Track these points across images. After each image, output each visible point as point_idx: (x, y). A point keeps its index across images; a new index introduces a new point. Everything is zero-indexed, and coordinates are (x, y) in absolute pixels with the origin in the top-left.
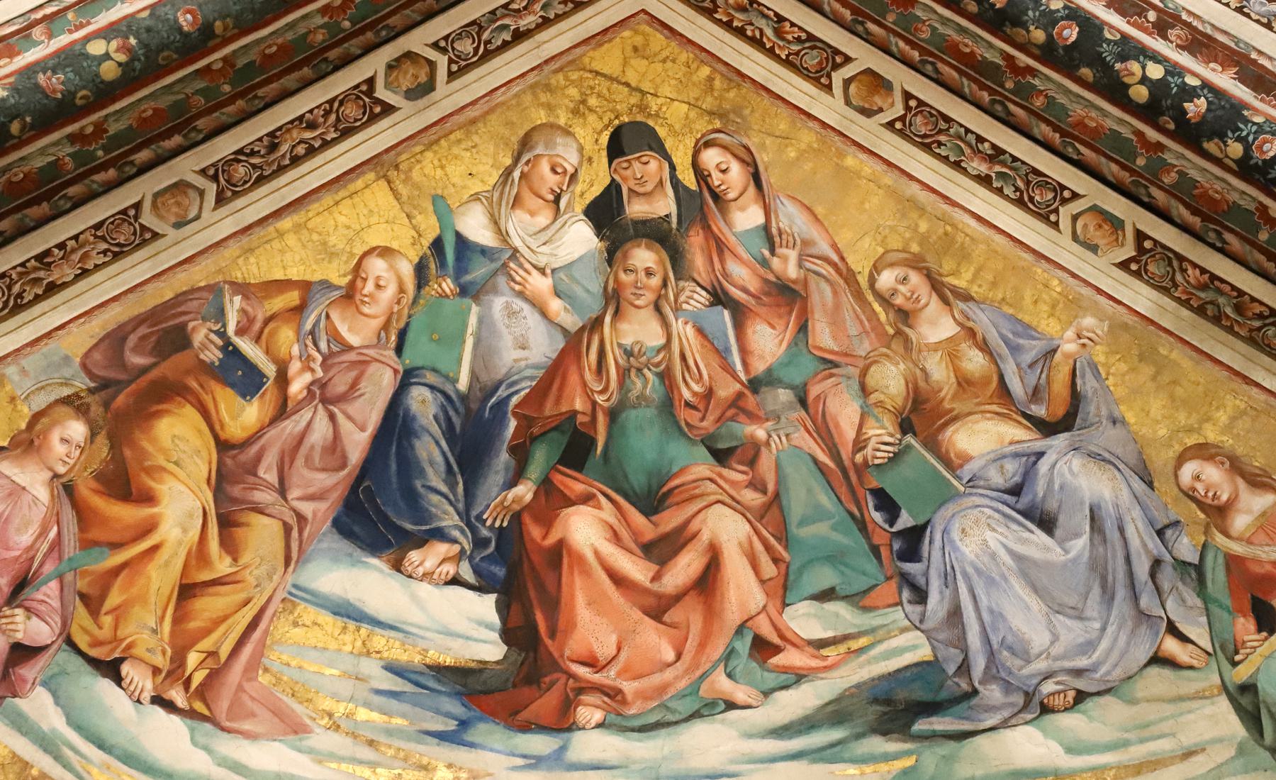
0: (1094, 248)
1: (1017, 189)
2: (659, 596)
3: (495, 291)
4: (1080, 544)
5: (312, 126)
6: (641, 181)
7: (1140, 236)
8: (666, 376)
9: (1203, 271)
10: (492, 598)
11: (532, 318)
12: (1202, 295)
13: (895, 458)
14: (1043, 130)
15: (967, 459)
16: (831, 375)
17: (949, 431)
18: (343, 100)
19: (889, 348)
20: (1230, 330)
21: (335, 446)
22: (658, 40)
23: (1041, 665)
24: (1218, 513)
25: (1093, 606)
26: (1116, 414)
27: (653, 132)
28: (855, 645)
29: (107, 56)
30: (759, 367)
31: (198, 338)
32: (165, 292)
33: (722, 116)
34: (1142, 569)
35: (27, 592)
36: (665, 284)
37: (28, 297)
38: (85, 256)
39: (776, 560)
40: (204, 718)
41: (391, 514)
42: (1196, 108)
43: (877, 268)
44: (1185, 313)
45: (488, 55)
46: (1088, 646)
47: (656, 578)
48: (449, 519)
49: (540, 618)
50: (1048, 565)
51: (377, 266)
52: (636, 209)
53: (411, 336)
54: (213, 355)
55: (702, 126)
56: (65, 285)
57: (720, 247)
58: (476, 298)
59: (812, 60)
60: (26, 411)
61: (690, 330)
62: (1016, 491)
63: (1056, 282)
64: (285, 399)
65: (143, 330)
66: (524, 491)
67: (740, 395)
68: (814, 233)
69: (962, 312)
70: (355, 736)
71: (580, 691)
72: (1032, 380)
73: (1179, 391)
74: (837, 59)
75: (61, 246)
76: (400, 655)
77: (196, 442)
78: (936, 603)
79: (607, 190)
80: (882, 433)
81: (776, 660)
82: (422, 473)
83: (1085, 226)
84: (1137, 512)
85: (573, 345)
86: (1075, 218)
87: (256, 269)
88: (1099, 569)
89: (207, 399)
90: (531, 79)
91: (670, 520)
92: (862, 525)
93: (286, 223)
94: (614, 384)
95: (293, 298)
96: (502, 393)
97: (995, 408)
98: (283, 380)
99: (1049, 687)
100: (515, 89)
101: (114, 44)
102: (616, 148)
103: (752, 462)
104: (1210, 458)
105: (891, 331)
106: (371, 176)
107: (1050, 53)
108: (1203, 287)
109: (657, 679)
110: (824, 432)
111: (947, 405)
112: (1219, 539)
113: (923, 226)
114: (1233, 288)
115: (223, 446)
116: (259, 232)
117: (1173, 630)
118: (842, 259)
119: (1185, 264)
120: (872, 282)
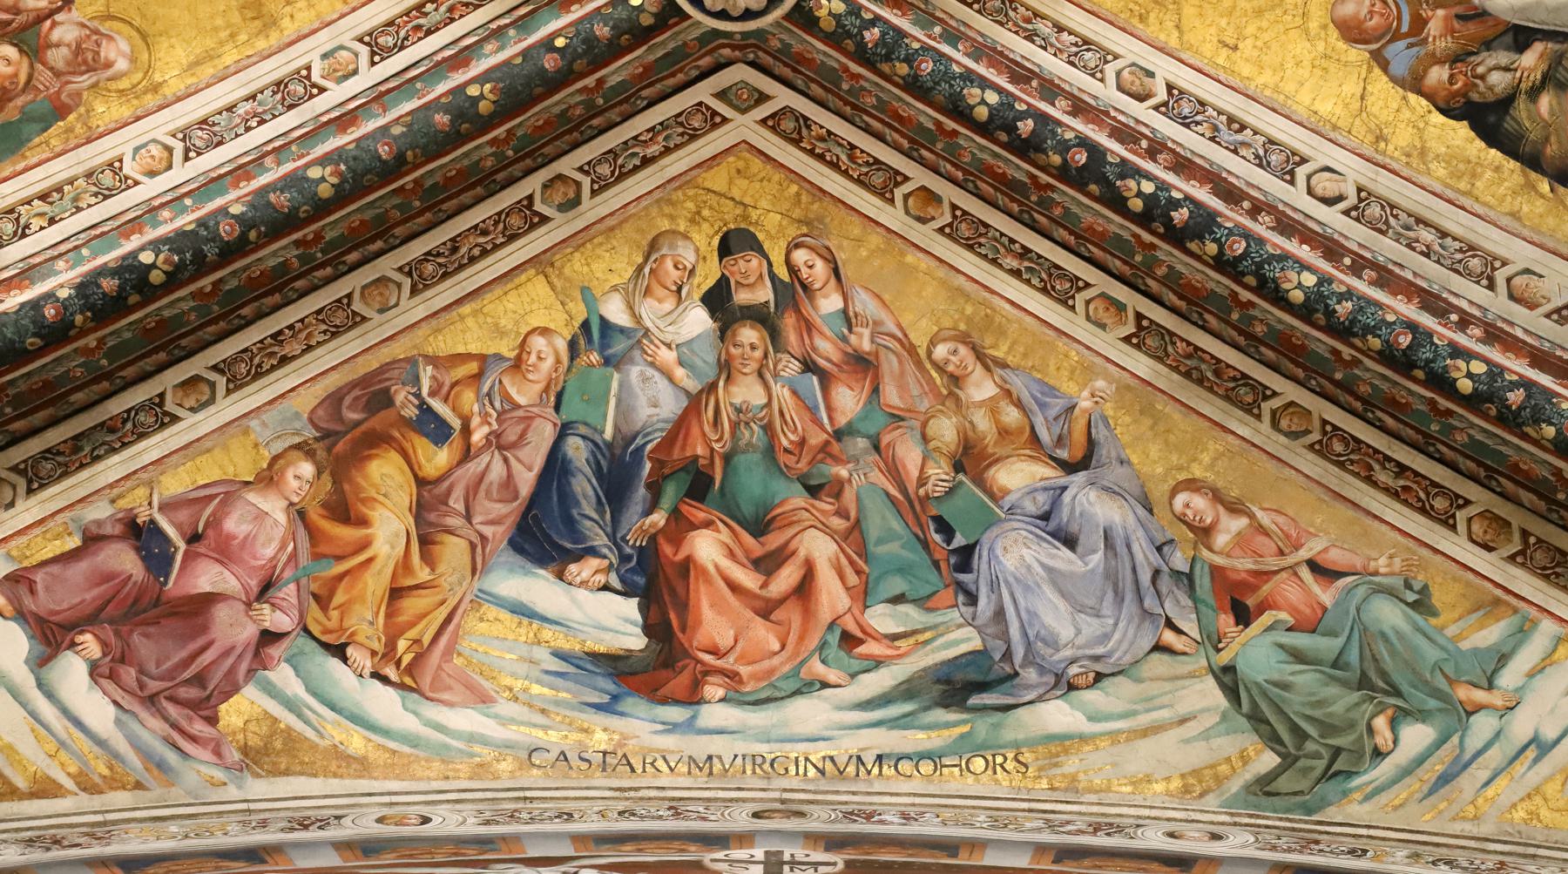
0: (1103, 326)
1: (1042, 280)
2: (767, 600)
3: (632, 362)
4: (1097, 558)
5: (485, 233)
6: (745, 275)
7: (1139, 317)
8: (768, 428)
9: (1189, 344)
10: (634, 602)
11: (661, 383)
12: (1189, 362)
13: (950, 492)
14: (1061, 234)
15: (1006, 492)
16: (900, 427)
17: (992, 471)
18: (508, 212)
19: (943, 405)
20: (1211, 390)
21: (509, 482)
22: (757, 164)
23: (1068, 653)
24: (1204, 533)
25: (1108, 607)
26: (1123, 456)
27: (754, 236)
28: (921, 638)
29: (323, 179)
30: (842, 421)
31: (400, 398)
32: (372, 363)
33: (808, 223)
34: (1145, 577)
35: (271, 592)
36: (766, 356)
37: (266, 367)
38: (309, 335)
39: (858, 572)
40: (412, 690)
41: (555, 537)
42: (1180, 216)
43: (933, 343)
44: (1175, 376)
45: (622, 177)
46: (1106, 637)
47: (764, 585)
48: (600, 540)
49: (673, 616)
50: (1072, 575)
51: (538, 342)
52: (742, 297)
53: (566, 398)
54: (411, 412)
55: (792, 231)
56: (294, 358)
57: (808, 327)
58: (617, 367)
59: (878, 179)
60: (267, 455)
61: (786, 392)
62: (1046, 517)
63: (1074, 353)
64: (468, 447)
65: (357, 392)
66: (659, 518)
67: (827, 443)
68: (883, 315)
69: (1002, 378)
70: (531, 706)
71: (706, 673)
72: (1056, 430)
73: (1172, 438)
74: (898, 178)
75: (291, 327)
76: (564, 644)
77: (399, 478)
78: (983, 601)
79: (719, 281)
80: (939, 472)
81: (861, 650)
82: (578, 503)
83: (1096, 308)
84: (1140, 533)
85: (695, 404)
86: (1088, 303)
87: (444, 344)
88: (1111, 576)
89: (407, 446)
90: (657, 195)
91: (774, 540)
92: (925, 544)
93: (466, 309)
94: (727, 435)
95: (473, 367)
96: (639, 441)
97: (1028, 452)
98: (466, 430)
99: (1074, 670)
100: (644, 203)
101: (328, 170)
102: (725, 249)
103: (838, 495)
104: (1197, 490)
105: (945, 392)
106: (532, 272)
107: (1064, 173)
108: (1189, 356)
109: (766, 664)
110: (894, 471)
111: (990, 450)
112: (1205, 553)
113: (969, 310)
114: (1213, 357)
115: (421, 482)
116: (445, 316)
117: (1170, 624)
118: (906, 335)
119: (1175, 339)
120: (929, 353)
